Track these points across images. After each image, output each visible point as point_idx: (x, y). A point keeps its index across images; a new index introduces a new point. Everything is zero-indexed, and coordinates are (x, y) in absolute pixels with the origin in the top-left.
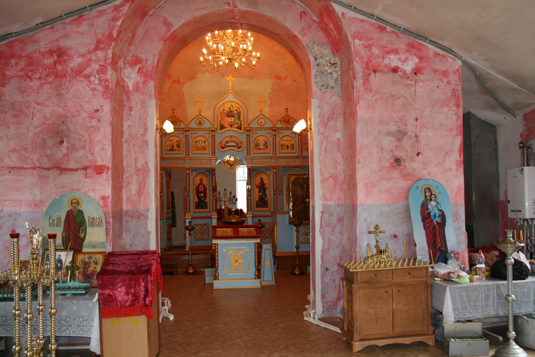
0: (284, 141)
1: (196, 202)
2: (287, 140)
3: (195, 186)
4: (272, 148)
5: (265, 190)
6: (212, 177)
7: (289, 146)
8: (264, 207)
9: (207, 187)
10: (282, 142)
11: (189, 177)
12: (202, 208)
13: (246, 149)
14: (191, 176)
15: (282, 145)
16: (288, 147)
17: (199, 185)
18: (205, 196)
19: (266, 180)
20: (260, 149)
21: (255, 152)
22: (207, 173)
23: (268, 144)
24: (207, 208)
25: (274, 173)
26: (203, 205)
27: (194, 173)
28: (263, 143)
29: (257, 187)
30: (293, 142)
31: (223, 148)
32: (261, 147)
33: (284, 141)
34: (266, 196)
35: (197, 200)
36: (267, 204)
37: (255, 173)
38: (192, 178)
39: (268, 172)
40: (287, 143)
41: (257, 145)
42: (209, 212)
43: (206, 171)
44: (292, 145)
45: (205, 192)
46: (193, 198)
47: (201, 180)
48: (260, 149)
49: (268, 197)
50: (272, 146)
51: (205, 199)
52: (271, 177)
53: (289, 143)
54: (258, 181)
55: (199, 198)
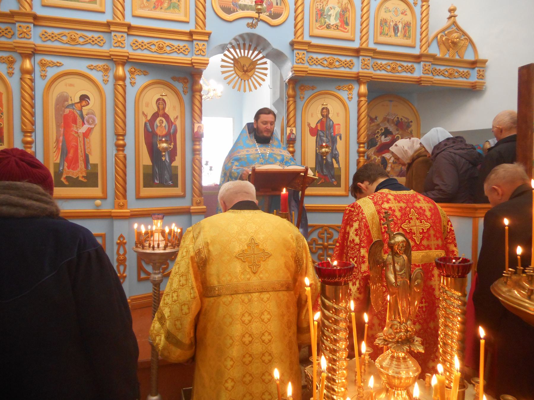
0: (388, 10)
1: (145, 167)
2: (396, 11)
3: (143, 121)
4: (358, 28)
5: (333, 141)
6: (193, 97)
7: (400, 26)
8: (331, 185)
9: (178, 123)
10: (383, 15)
11: (124, 88)
12: (163, 184)
13: (291, 22)
14: (129, 87)
15: (384, 22)
16: (396, 29)
17: (155, 116)
18: (173, 154)
19: (336, 115)
20: (328, 27)
21: (317, 32)
22: (179, 86)
23: (349, 14)
24: (175, 185)
25: (360, 95)
26: (167, 176)
27: (141, 81)
28: (338, 9)
29: (313, 132)
30: (408, 18)
31: (228, 11)
32: (333, 21)
33: (388, 10)
34: (336, 157)
35: (146, 160)
36: (339, 178)
37: (308, 94)
38: (131, 93)
39: (344, 95)
40: (397, 19)
41: (321, 14)
42: (183, 196)
43: (174, 79)
44: (407, 25)
45: (171, 137)
46: (137, 156)
47: (161, 102)
48: (328, 27)
49: (341, 158)
50: (358, 21)
51: (172, 159)
52: (353, 106)
53: (401, 20)
54: (314, 118)
55: (154, 152)
